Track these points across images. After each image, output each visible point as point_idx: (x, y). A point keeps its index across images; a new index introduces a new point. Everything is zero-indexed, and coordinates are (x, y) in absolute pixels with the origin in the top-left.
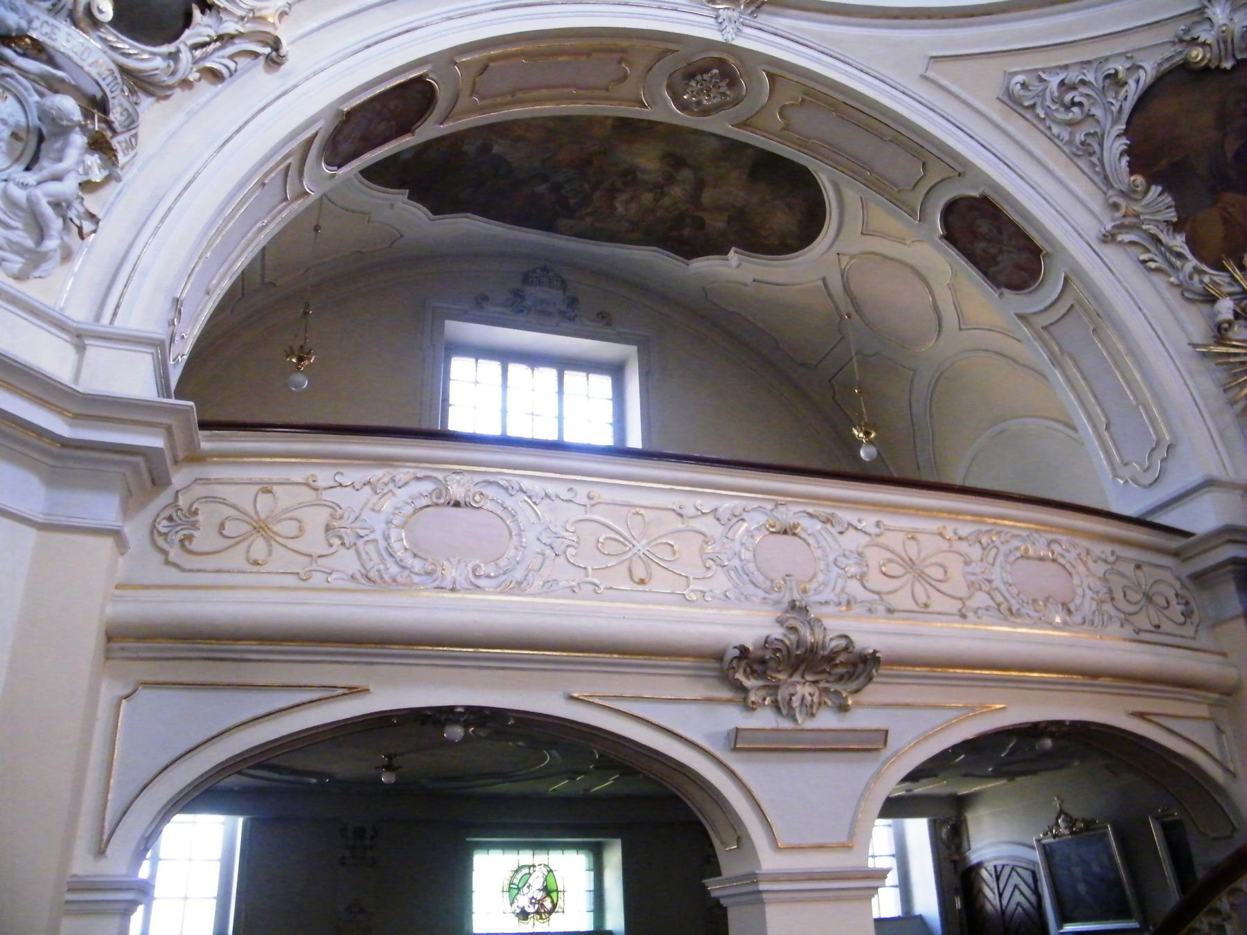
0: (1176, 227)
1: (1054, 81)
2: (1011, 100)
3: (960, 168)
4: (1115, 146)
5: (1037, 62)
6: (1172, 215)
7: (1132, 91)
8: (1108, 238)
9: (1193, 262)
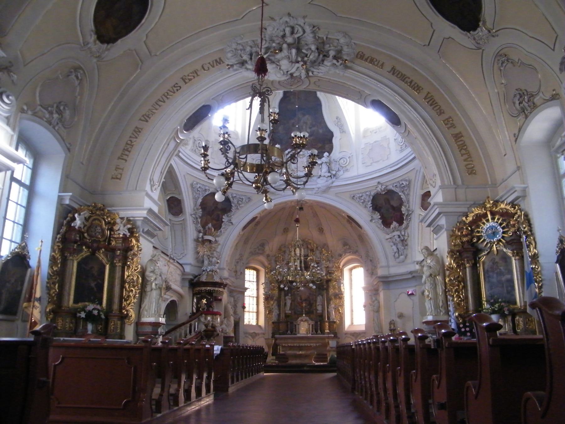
0: (200, 217)
1: (199, 186)
2: (192, 185)
3: (180, 193)
4: (200, 200)
5: (198, 181)
6: (200, 215)
7: (207, 193)
8: (191, 215)
9: (199, 225)
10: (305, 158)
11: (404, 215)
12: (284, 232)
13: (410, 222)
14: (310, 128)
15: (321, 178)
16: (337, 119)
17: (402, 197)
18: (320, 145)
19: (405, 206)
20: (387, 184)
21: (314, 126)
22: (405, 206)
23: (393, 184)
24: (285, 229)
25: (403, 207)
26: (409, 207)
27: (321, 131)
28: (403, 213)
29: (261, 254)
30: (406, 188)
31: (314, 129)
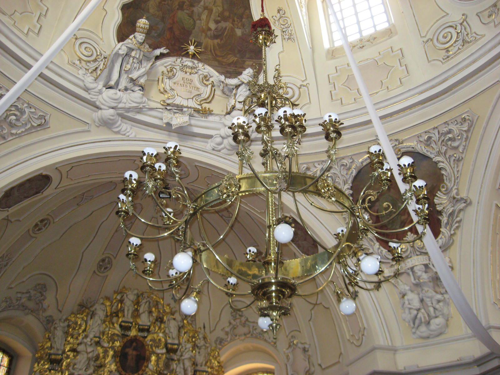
10: (196, 75)
11: (440, 213)
12: (100, 267)
13: (459, 232)
14: (217, 22)
15: (234, 113)
16: (279, 11)
17: (441, 165)
18: (232, 59)
19: (448, 192)
20: (401, 137)
21: (225, 19)
22: (448, 192)
23: (419, 136)
24: (103, 260)
25: (439, 194)
26: (457, 194)
27: (239, 32)
28: (439, 208)
29: (32, 311)
30: (455, 144)
31: (223, 24)
